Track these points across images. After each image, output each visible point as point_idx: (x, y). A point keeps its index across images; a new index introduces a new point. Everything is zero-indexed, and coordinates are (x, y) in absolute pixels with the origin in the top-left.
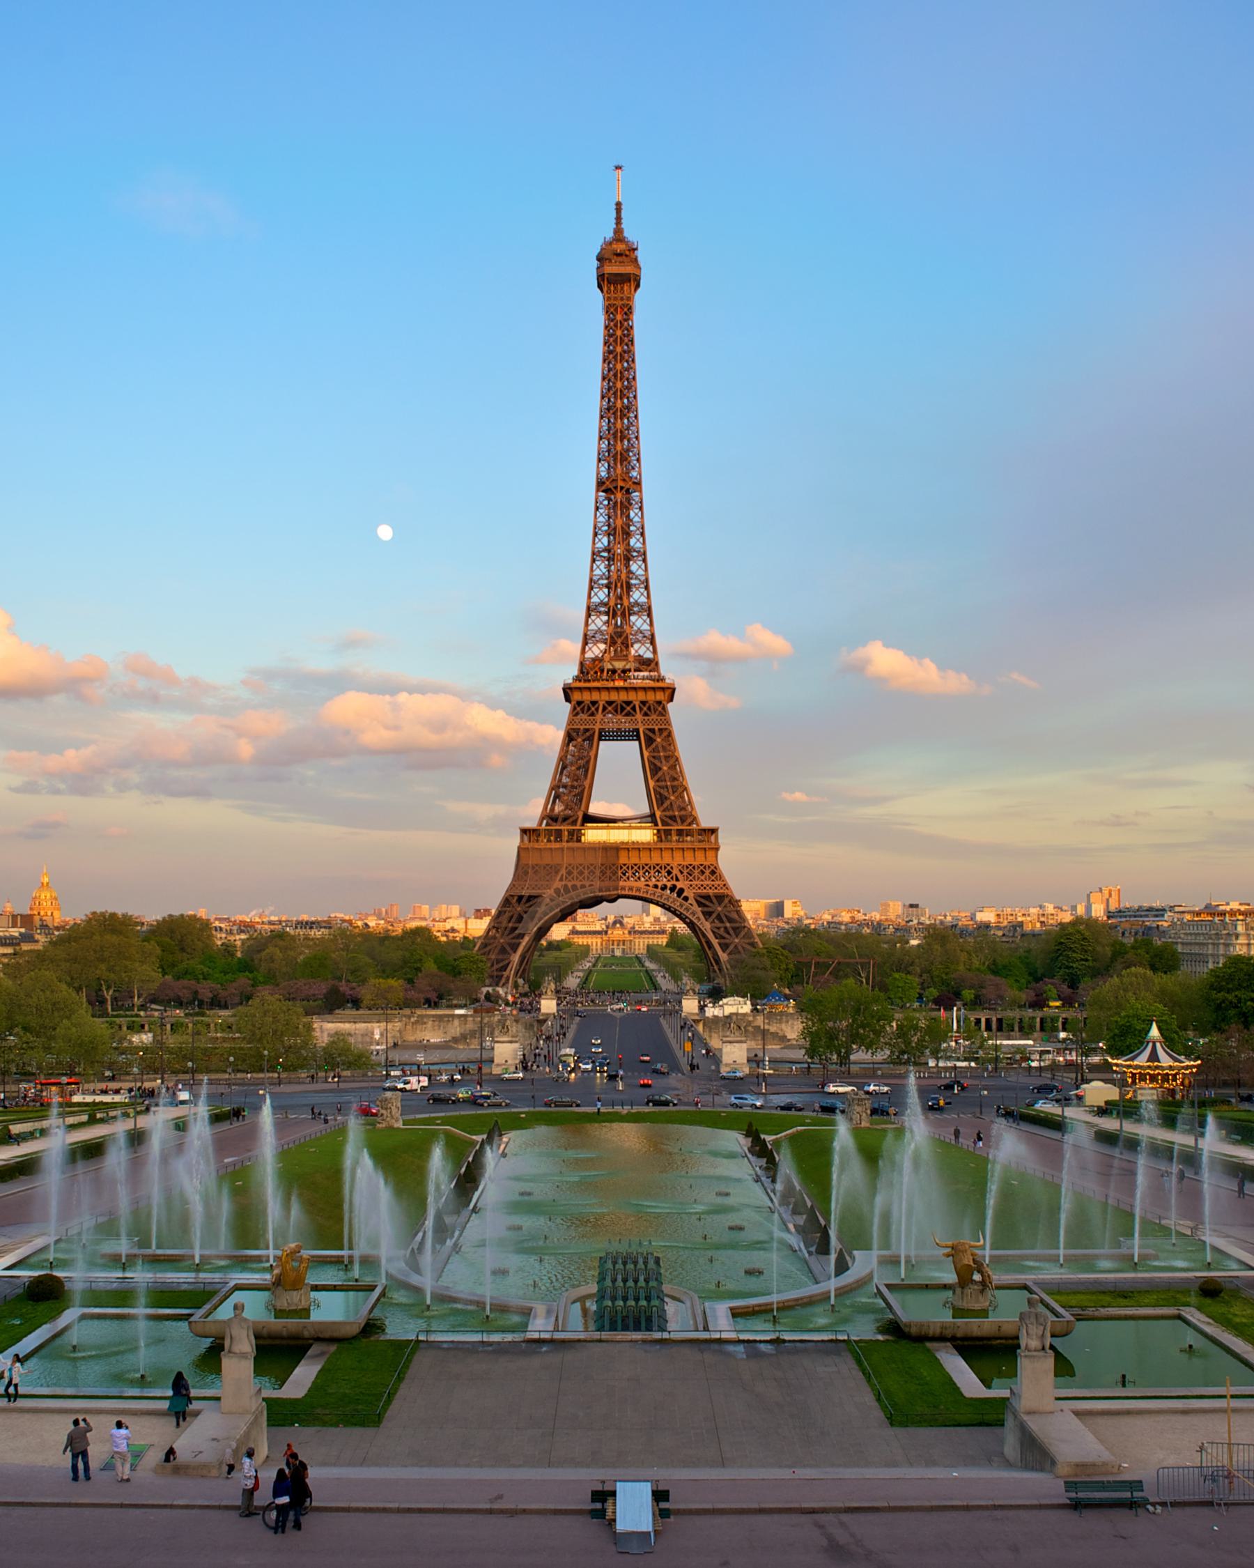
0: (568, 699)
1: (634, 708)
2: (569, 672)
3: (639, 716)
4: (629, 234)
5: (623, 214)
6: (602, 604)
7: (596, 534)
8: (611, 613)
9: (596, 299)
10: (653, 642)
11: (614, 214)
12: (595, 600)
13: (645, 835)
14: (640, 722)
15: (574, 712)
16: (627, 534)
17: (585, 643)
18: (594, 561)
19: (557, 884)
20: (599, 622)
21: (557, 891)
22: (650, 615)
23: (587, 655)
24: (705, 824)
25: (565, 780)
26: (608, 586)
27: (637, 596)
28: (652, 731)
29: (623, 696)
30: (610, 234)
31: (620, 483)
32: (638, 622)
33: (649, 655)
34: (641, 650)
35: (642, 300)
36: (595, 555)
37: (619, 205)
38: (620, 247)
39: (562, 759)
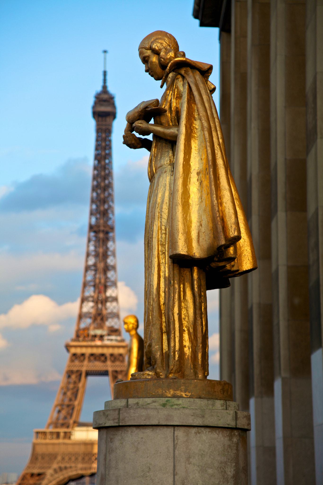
0: (68, 350)
1: (106, 358)
3: (109, 363)
4: (111, 89)
5: (108, 77)
9: (92, 123)
11: (101, 77)
14: (109, 366)
16: (105, 256)
19: (55, 466)
26: (94, 286)
28: (116, 372)
29: (99, 351)
30: (99, 88)
31: (102, 228)
37: (105, 73)
38: (105, 97)
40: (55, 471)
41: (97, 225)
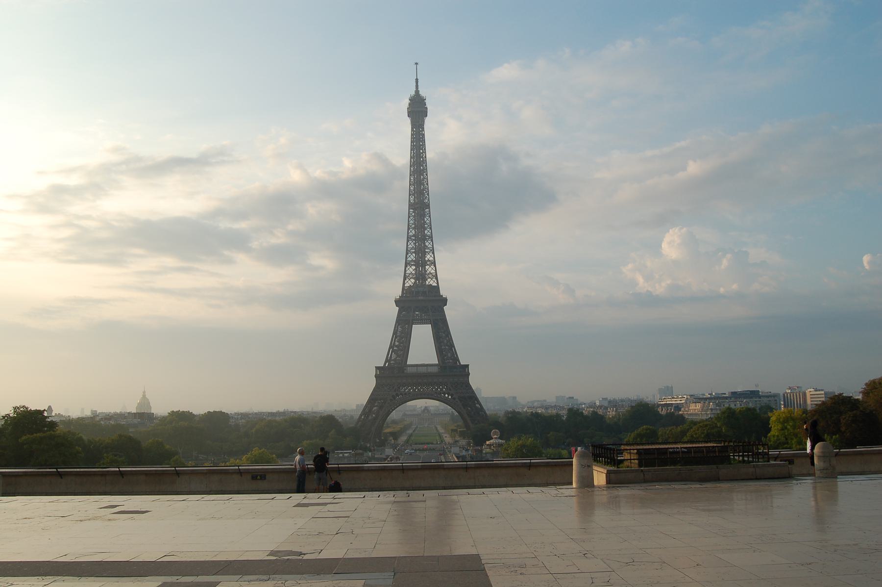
6: (412, 261)
7: (409, 229)
8: (417, 265)
10: (437, 279)
12: (409, 259)
13: (435, 370)
15: (400, 312)
18: (408, 241)
20: (411, 270)
22: (435, 266)
23: (407, 285)
24: (463, 362)
25: (397, 343)
27: (429, 257)
30: (413, 93)
32: (430, 269)
34: (431, 282)
36: (409, 238)
37: (417, 80)
39: (395, 333)
41: (415, 203)
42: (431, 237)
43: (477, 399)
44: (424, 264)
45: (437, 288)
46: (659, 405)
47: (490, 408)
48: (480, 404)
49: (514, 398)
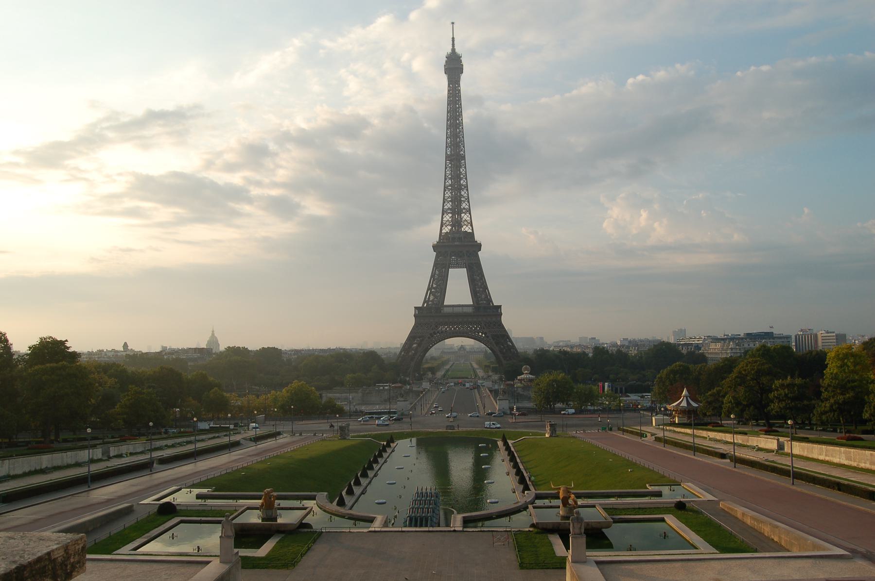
2: (436, 239)
4: (458, 50)
8: (453, 213)
10: (472, 226)
13: (470, 310)
17: (442, 226)
18: (445, 191)
20: (448, 217)
21: (431, 334)
30: (450, 51)
32: (465, 217)
33: (470, 231)
34: (466, 229)
35: (463, 77)
39: (433, 276)
40: (431, 334)
41: (451, 155)
42: (466, 187)
43: (508, 337)
44: (460, 212)
45: (472, 234)
46: (679, 345)
47: (520, 346)
48: (512, 342)
49: (542, 338)
